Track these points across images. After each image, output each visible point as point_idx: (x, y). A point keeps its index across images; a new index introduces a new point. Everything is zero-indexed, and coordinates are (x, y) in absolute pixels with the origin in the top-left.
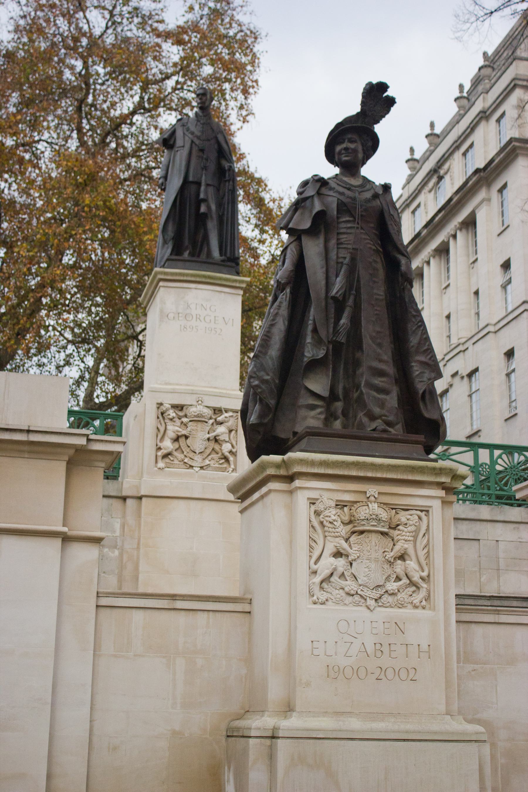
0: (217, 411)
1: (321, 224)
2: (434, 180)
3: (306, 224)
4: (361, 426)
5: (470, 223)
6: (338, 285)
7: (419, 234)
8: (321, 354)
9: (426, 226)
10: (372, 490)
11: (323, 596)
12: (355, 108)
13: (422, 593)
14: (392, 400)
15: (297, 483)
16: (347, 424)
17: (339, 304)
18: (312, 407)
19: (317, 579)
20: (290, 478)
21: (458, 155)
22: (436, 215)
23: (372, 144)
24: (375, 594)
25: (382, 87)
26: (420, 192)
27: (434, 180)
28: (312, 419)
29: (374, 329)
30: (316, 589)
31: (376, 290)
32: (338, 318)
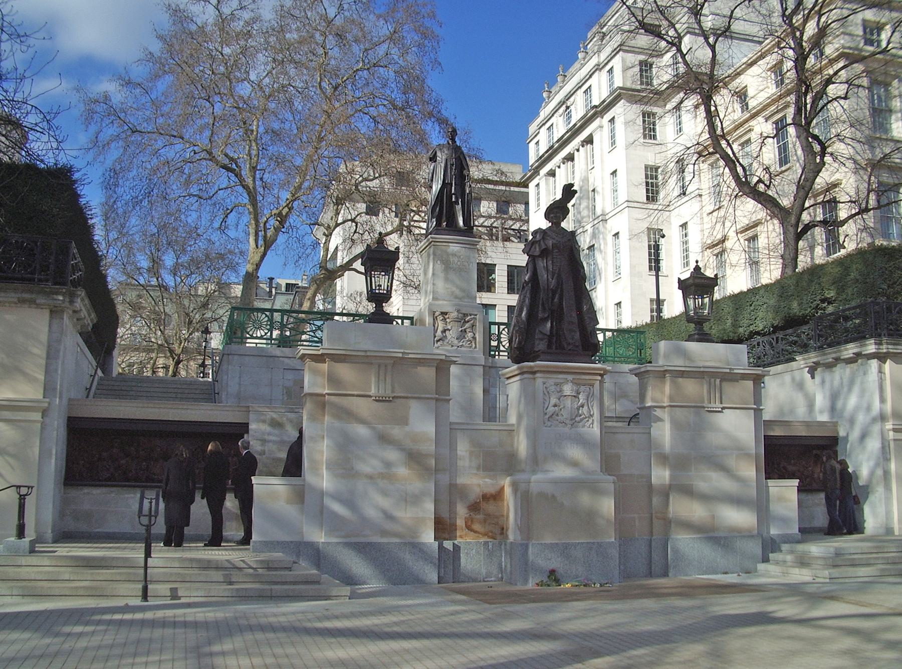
0: (465, 315)
1: (545, 253)
2: (563, 108)
3: (537, 253)
4: (564, 348)
5: (589, 141)
6: (553, 283)
7: (552, 146)
8: (546, 315)
9: (557, 141)
10: (570, 377)
11: (549, 424)
12: (559, 196)
13: (591, 421)
14: (577, 335)
15: (538, 375)
16: (558, 348)
17: (554, 292)
18: (542, 340)
19: (547, 417)
20: (534, 373)
21: (580, 92)
22: (565, 134)
23: (566, 212)
24: (571, 422)
25: (572, 185)
26: (553, 115)
27: (563, 108)
28: (541, 346)
29: (568, 303)
30: (546, 421)
31: (568, 286)
32: (553, 299)
